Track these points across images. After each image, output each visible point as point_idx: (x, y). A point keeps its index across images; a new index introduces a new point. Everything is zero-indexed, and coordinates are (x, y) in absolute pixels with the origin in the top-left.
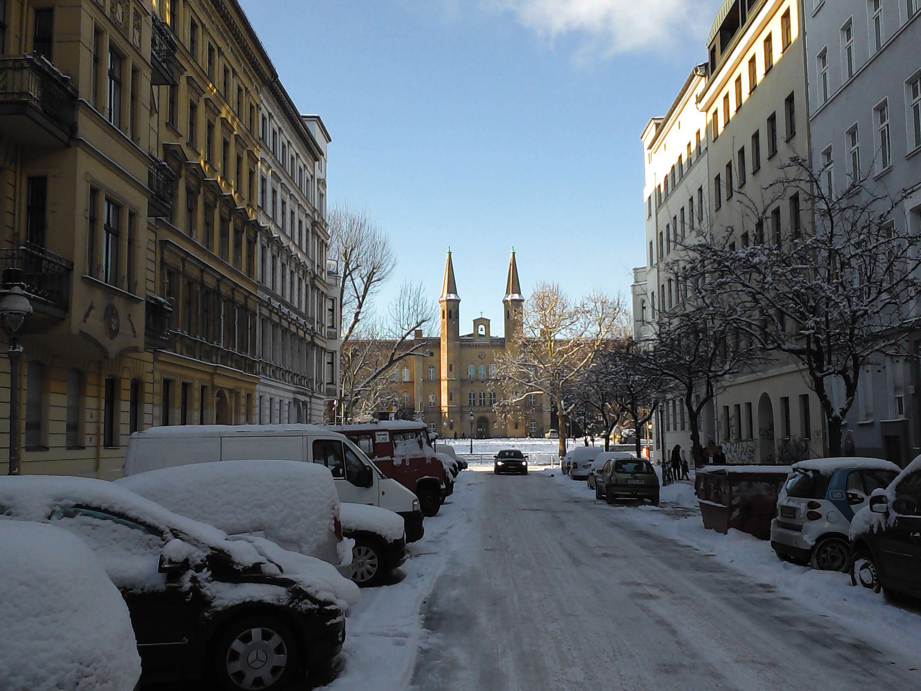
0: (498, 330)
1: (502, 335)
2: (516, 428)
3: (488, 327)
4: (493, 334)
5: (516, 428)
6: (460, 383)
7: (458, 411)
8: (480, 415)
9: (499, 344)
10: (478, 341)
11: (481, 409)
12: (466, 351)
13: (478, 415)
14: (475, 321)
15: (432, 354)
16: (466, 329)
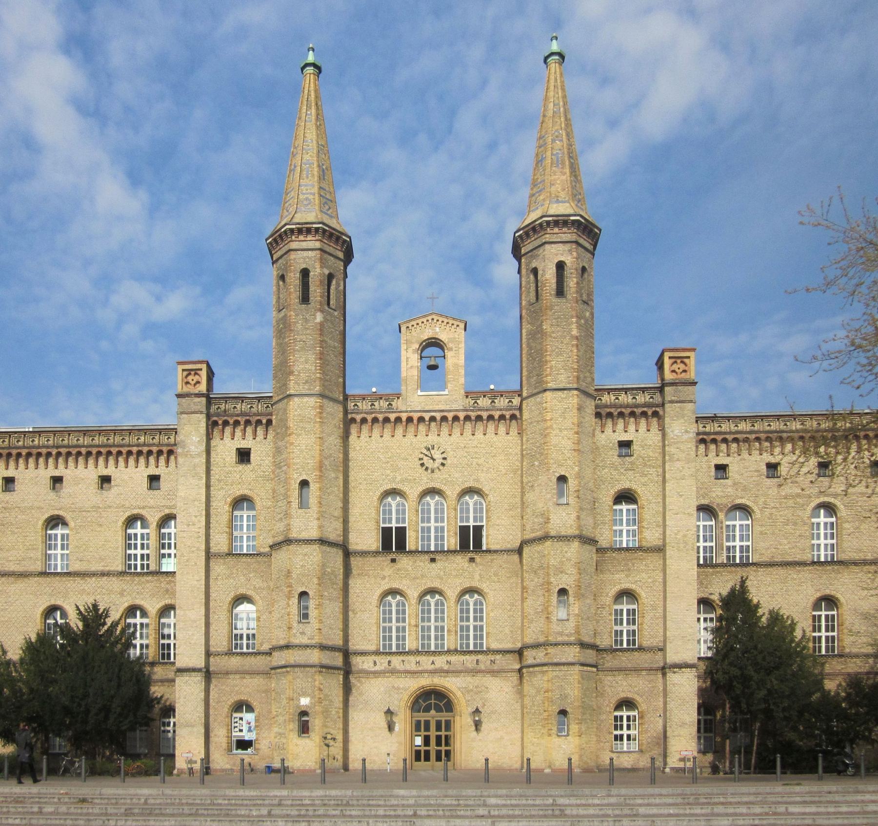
8: (425, 682)
11: (426, 662)
13: (414, 685)
15: (244, 456)
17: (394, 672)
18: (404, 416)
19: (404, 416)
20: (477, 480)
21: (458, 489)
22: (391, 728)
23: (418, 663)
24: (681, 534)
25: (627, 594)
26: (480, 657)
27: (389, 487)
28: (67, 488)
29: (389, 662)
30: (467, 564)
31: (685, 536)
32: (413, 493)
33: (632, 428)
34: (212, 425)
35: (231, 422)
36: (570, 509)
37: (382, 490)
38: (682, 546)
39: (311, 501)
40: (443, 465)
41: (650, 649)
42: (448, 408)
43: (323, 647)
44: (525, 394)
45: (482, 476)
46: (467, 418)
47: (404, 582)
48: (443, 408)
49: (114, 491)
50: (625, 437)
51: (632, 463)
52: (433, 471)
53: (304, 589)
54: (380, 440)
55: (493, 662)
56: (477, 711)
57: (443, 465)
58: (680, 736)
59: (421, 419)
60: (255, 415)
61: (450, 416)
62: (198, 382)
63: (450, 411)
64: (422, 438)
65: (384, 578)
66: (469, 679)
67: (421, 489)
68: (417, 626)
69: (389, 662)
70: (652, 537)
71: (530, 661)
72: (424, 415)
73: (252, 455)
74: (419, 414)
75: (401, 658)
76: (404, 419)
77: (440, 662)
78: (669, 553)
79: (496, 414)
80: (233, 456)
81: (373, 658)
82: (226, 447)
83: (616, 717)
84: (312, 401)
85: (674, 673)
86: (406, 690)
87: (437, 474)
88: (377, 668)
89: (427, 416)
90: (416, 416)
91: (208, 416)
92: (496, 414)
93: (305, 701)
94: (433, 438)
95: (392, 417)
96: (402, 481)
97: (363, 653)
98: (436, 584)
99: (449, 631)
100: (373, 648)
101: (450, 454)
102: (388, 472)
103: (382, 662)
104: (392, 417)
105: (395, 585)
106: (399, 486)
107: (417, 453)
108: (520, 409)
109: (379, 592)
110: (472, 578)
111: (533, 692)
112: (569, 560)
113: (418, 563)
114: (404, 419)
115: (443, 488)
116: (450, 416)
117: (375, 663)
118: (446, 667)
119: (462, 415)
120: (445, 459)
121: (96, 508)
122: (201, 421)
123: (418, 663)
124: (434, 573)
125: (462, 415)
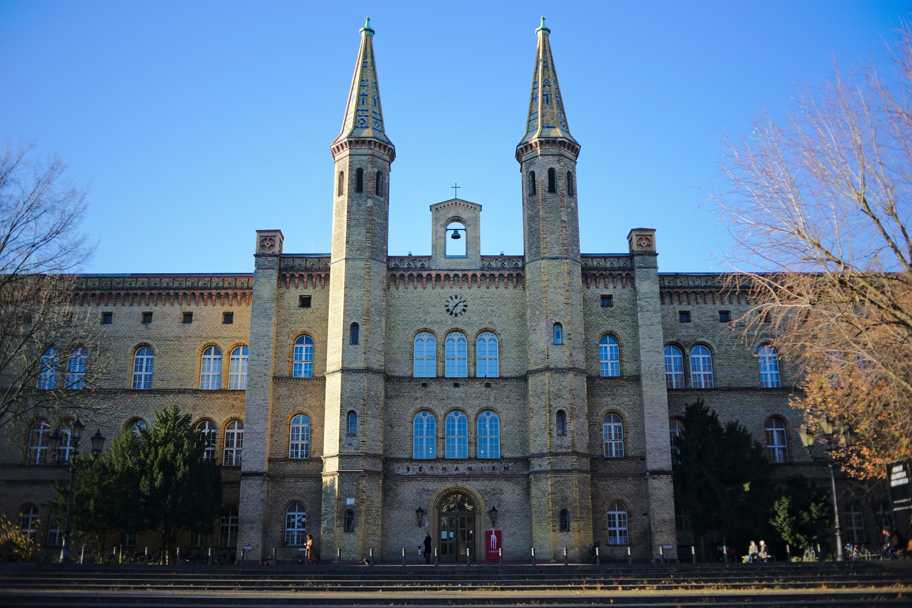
0: (503, 233)
1: (515, 247)
2: (564, 527)
3: (472, 225)
4: (489, 247)
5: (564, 527)
6: (383, 384)
7: (376, 467)
8: (450, 485)
9: (509, 271)
10: (443, 264)
12: (409, 295)
13: (441, 487)
14: (435, 208)
15: (305, 302)
16: (409, 236)
17: (423, 476)
18: (434, 273)
19: (434, 273)
20: (491, 323)
21: (477, 330)
22: (420, 524)
23: (444, 469)
24: (653, 367)
25: (615, 415)
26: (496, 464)
27: (421, 327)
28: (155, 322)
29: (420, 468)
30: (484, 389)
31: (656, 369)
32: (440, 331)
33: (611, 286)
34: (282, 278)
35: (297, 275)
36: (564, 348)
37: (415, 329)
38: (654, 376)
39: (360, 339)
40: (464, 310)
41: (633, 458)
42: (468, 268)
43: (367, 456)
44: (527, 260)
45: (495, 319)
46: (483, 275)
47: (433, 402)
48: (464, 268)
49: (194, 324)
50: (606, 292)
51: (612, 312)
52: (456, 315)
53: (352, 409)
54: (415, 291)
55: (506, 468)
56: (494, 509)
57: (464, 310)
58: (661, 531)
59: (447, 276)
60: (316, 270)
61: (470, 274)
62: (272, 245)
63: (469, 270)
64: (448, 291)
65: (416, 399)
66: (487, 483)
67: (446, 329)
68: (443, 438)
69: (420, 468)
70: (629, 368)
71: (537, 468)
72: (449, 273)
73: (312, 301)
74: (446, 273)
75: (430, 465)
76: (434, 276)
77: (463, 468)
78: (644, 381)
79: (506, 273)
80: (297, 302)
81: (407, 464)
82: (293, 294)
83: (609, 516)
84: (362, 264)
85: (654, 478)
86: (434, 491)
87: (459, 318)
88: (410, 473)
89: (452, 274)
90: (443, 273)
91: (280, 270)
92: (506, 273)
93: (350, 501)
94: (456, 290)
95: (425, 274)
96: (432, 323)
97: (399, 460)
98: (460, 404)
99: (469, 443)
100: (407, 456)
101: (470, 303)
102: (421, 315)
103: (414, 469)
104: (425, 274)
105: (426, 405)
106: (429, 327)
107: (444, 301)
108: (523, 268)
109: (412, 410)
110: (488, 399)
111: (540, 494)
112: (565, 387)
113: (445, 387)
114: (434, 276)
115: (464, 328)
116: (470, 274)
117: (408, 469)
118: (468, 473)
119: (479, 274)
120: (465, 306)
121: (178, 338)
122: (275, 274)
123: (444, 469)
124: (457, 396)
125: (479, 274)
